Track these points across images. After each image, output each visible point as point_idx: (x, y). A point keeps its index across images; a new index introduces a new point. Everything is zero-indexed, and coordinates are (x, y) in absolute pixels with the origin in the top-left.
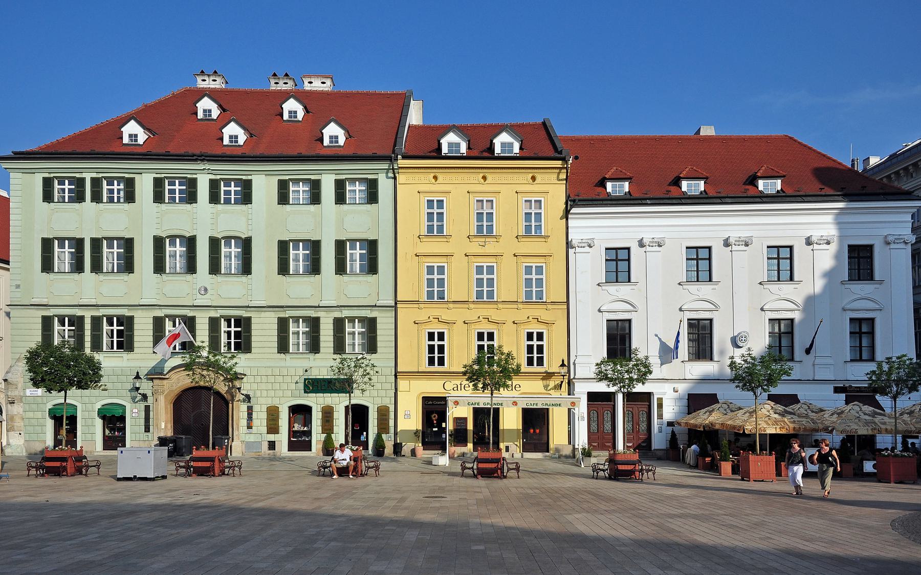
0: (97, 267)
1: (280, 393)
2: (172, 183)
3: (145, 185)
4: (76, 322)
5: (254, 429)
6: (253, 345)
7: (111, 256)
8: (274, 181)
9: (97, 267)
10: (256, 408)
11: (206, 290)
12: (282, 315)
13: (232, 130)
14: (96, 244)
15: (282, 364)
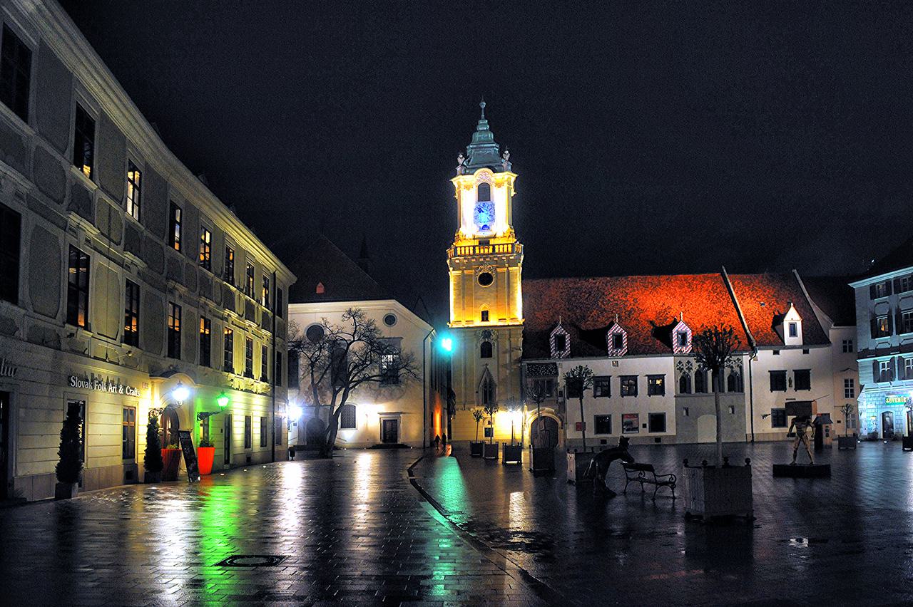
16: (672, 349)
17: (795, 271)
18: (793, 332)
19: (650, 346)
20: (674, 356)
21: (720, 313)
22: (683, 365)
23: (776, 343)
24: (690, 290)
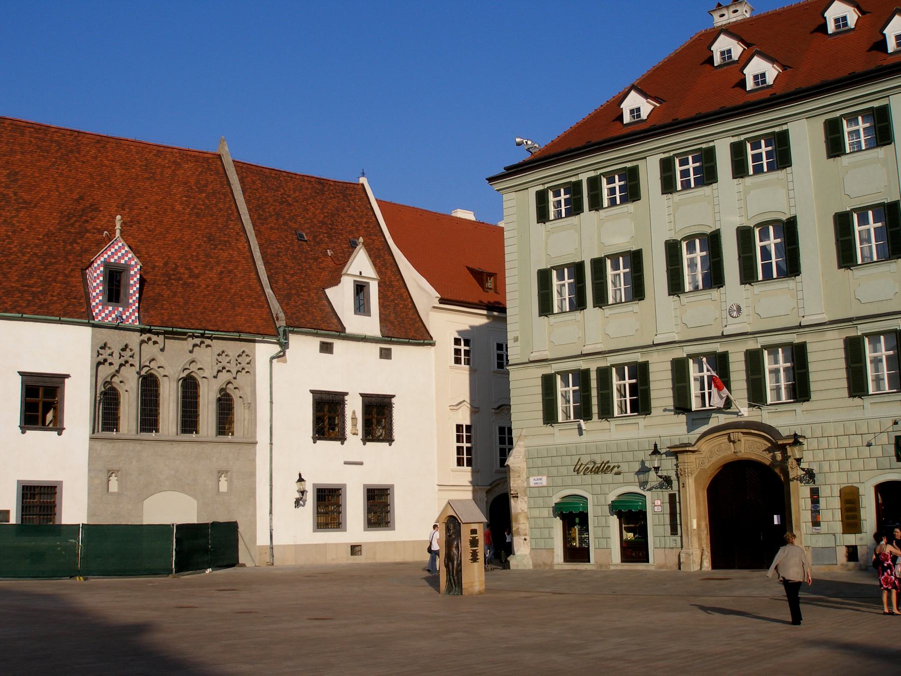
0: (601, 300)
1: (859, 464)
2: (684, 162)
3: (650, 175)
4: (582, 377)
5: (824, 527)
6: (813, 387)
7: (616, 279)
8: (819, 125)
9: (601, 300)
10: (824, 492)
11: (739, 309)
12: (852, 333)
13: (758, 66)
14: (598, 265)
15: (857, 414)
16: (89, 310)
17: (363, 180)
18: (362, 307)
19: (34, 294)
20: (94, 326)
21: (210, 239)
22: (111, 355)
23: (328, 329)
24: (146, 175)
